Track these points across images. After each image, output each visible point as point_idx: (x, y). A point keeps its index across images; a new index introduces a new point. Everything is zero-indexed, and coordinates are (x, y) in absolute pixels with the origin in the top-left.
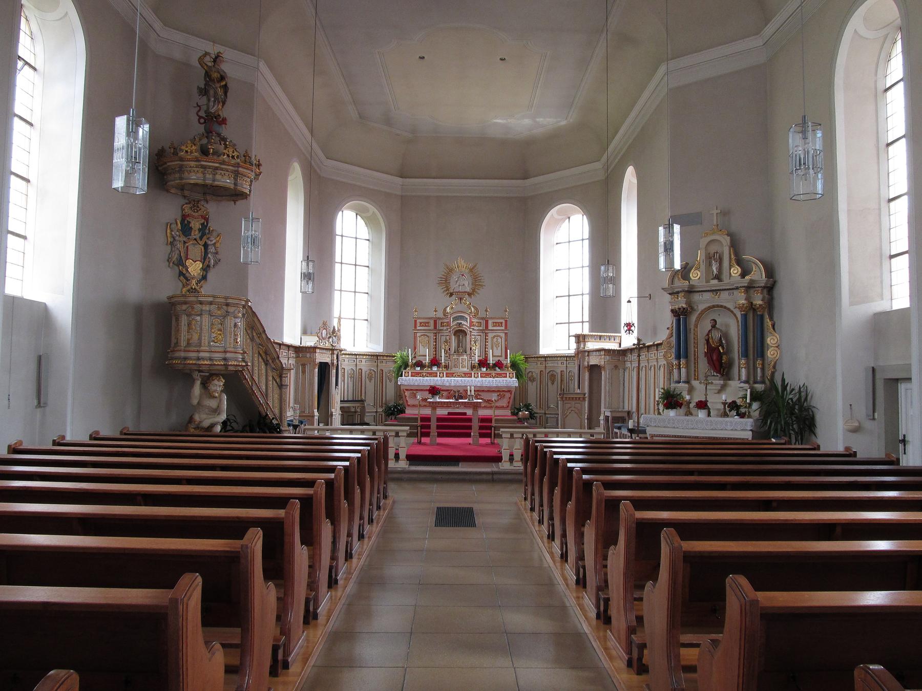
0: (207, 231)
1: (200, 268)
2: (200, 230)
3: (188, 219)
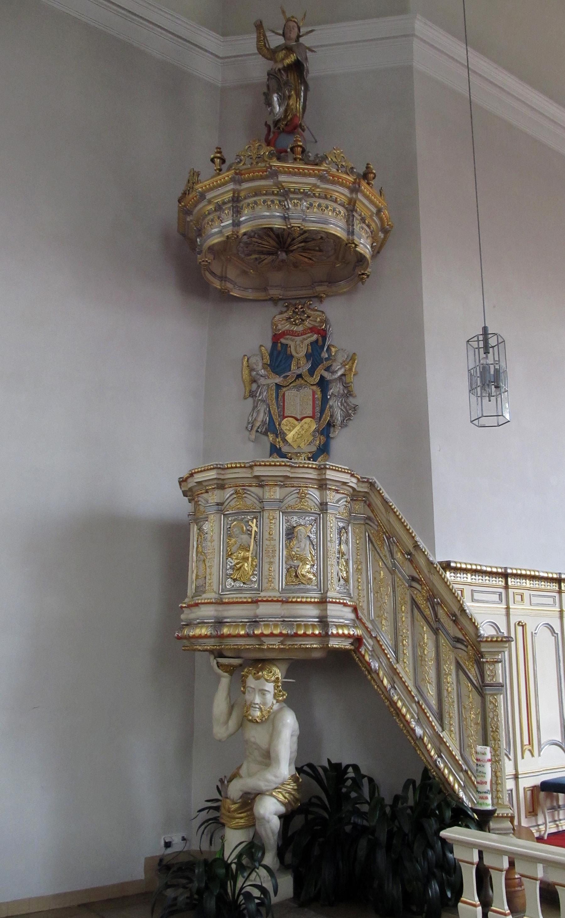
0: (325, 355)
2: (308, 356)
3: (283, 340)
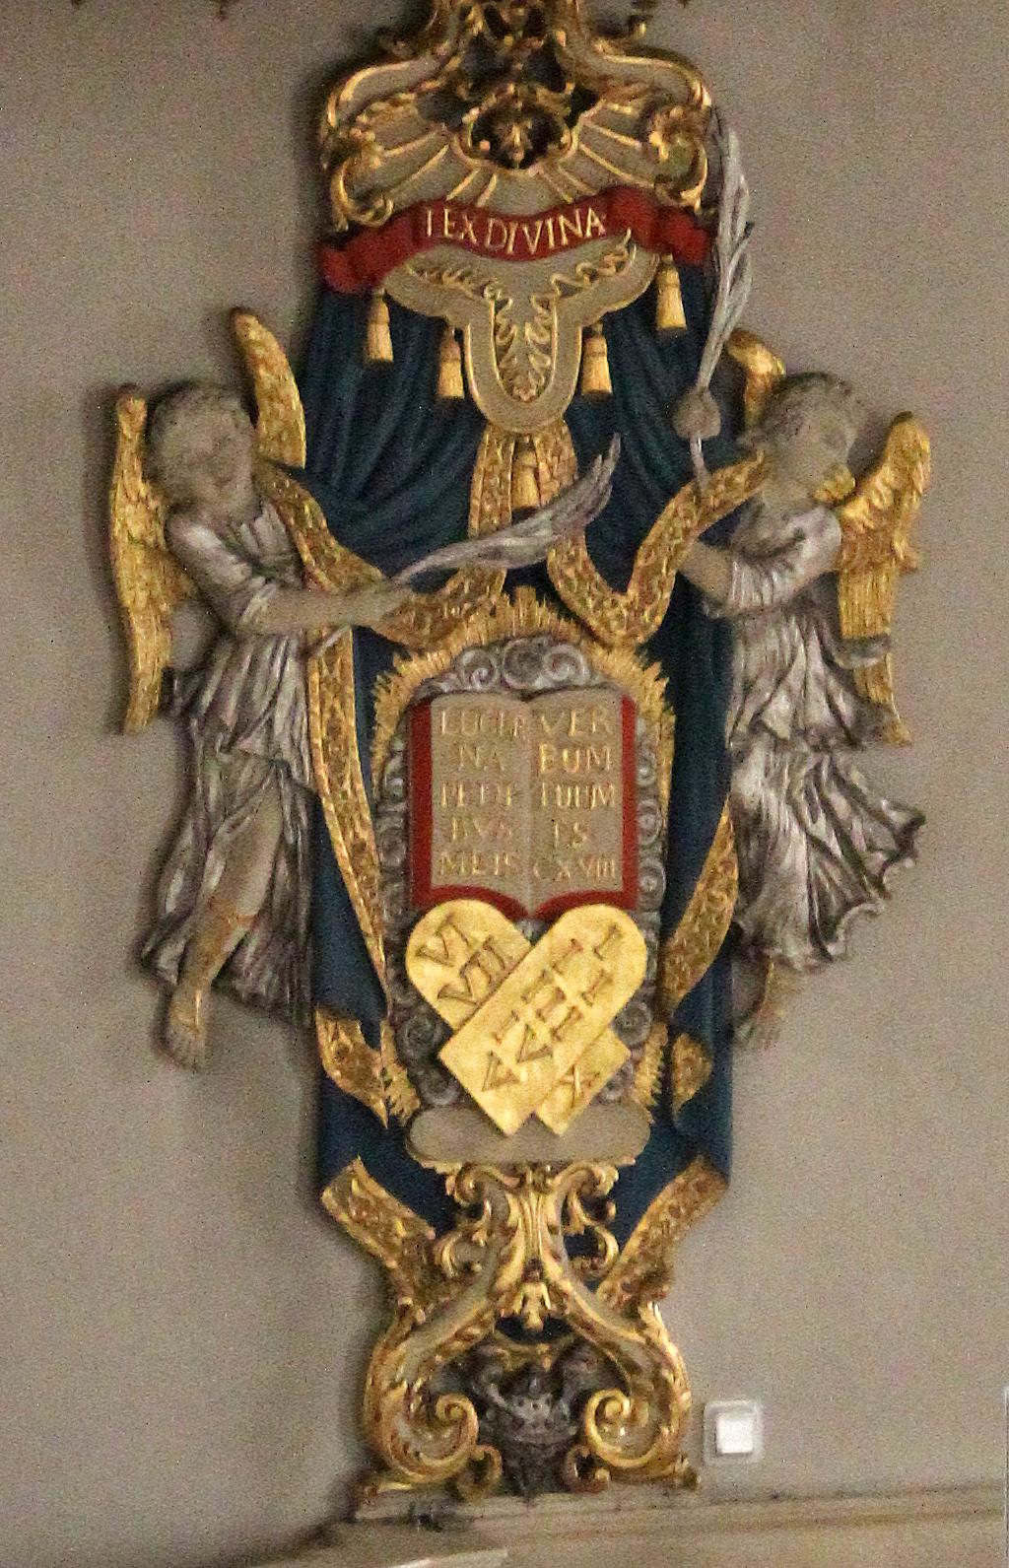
0: (701, 421)
1: (619, 998)
3: (405, 283)
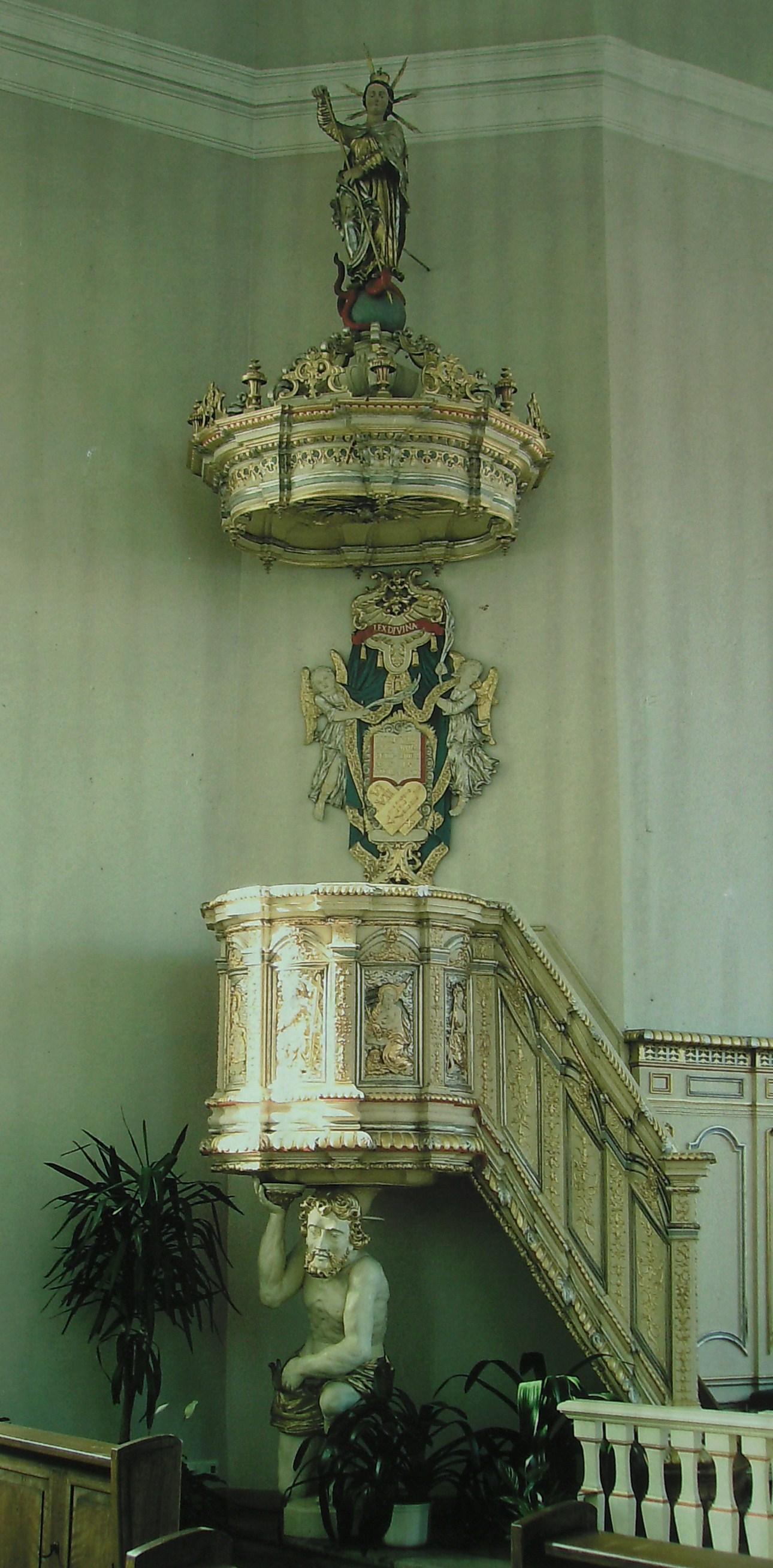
0: (441, 669)
2: (412, 671)
